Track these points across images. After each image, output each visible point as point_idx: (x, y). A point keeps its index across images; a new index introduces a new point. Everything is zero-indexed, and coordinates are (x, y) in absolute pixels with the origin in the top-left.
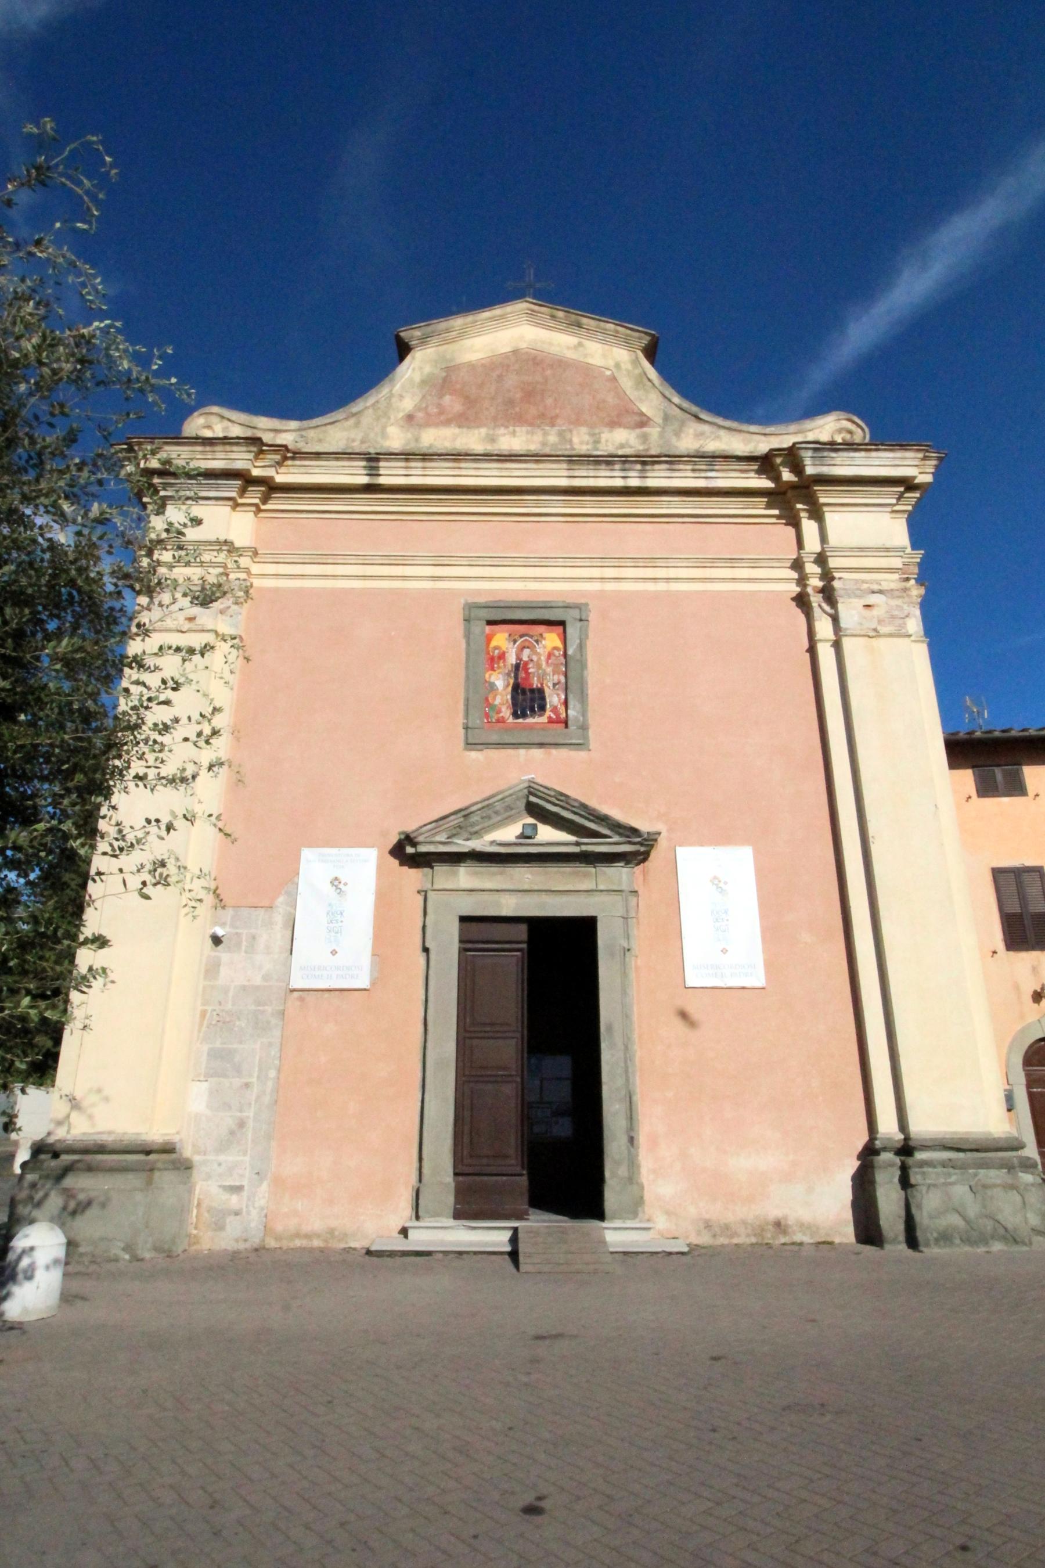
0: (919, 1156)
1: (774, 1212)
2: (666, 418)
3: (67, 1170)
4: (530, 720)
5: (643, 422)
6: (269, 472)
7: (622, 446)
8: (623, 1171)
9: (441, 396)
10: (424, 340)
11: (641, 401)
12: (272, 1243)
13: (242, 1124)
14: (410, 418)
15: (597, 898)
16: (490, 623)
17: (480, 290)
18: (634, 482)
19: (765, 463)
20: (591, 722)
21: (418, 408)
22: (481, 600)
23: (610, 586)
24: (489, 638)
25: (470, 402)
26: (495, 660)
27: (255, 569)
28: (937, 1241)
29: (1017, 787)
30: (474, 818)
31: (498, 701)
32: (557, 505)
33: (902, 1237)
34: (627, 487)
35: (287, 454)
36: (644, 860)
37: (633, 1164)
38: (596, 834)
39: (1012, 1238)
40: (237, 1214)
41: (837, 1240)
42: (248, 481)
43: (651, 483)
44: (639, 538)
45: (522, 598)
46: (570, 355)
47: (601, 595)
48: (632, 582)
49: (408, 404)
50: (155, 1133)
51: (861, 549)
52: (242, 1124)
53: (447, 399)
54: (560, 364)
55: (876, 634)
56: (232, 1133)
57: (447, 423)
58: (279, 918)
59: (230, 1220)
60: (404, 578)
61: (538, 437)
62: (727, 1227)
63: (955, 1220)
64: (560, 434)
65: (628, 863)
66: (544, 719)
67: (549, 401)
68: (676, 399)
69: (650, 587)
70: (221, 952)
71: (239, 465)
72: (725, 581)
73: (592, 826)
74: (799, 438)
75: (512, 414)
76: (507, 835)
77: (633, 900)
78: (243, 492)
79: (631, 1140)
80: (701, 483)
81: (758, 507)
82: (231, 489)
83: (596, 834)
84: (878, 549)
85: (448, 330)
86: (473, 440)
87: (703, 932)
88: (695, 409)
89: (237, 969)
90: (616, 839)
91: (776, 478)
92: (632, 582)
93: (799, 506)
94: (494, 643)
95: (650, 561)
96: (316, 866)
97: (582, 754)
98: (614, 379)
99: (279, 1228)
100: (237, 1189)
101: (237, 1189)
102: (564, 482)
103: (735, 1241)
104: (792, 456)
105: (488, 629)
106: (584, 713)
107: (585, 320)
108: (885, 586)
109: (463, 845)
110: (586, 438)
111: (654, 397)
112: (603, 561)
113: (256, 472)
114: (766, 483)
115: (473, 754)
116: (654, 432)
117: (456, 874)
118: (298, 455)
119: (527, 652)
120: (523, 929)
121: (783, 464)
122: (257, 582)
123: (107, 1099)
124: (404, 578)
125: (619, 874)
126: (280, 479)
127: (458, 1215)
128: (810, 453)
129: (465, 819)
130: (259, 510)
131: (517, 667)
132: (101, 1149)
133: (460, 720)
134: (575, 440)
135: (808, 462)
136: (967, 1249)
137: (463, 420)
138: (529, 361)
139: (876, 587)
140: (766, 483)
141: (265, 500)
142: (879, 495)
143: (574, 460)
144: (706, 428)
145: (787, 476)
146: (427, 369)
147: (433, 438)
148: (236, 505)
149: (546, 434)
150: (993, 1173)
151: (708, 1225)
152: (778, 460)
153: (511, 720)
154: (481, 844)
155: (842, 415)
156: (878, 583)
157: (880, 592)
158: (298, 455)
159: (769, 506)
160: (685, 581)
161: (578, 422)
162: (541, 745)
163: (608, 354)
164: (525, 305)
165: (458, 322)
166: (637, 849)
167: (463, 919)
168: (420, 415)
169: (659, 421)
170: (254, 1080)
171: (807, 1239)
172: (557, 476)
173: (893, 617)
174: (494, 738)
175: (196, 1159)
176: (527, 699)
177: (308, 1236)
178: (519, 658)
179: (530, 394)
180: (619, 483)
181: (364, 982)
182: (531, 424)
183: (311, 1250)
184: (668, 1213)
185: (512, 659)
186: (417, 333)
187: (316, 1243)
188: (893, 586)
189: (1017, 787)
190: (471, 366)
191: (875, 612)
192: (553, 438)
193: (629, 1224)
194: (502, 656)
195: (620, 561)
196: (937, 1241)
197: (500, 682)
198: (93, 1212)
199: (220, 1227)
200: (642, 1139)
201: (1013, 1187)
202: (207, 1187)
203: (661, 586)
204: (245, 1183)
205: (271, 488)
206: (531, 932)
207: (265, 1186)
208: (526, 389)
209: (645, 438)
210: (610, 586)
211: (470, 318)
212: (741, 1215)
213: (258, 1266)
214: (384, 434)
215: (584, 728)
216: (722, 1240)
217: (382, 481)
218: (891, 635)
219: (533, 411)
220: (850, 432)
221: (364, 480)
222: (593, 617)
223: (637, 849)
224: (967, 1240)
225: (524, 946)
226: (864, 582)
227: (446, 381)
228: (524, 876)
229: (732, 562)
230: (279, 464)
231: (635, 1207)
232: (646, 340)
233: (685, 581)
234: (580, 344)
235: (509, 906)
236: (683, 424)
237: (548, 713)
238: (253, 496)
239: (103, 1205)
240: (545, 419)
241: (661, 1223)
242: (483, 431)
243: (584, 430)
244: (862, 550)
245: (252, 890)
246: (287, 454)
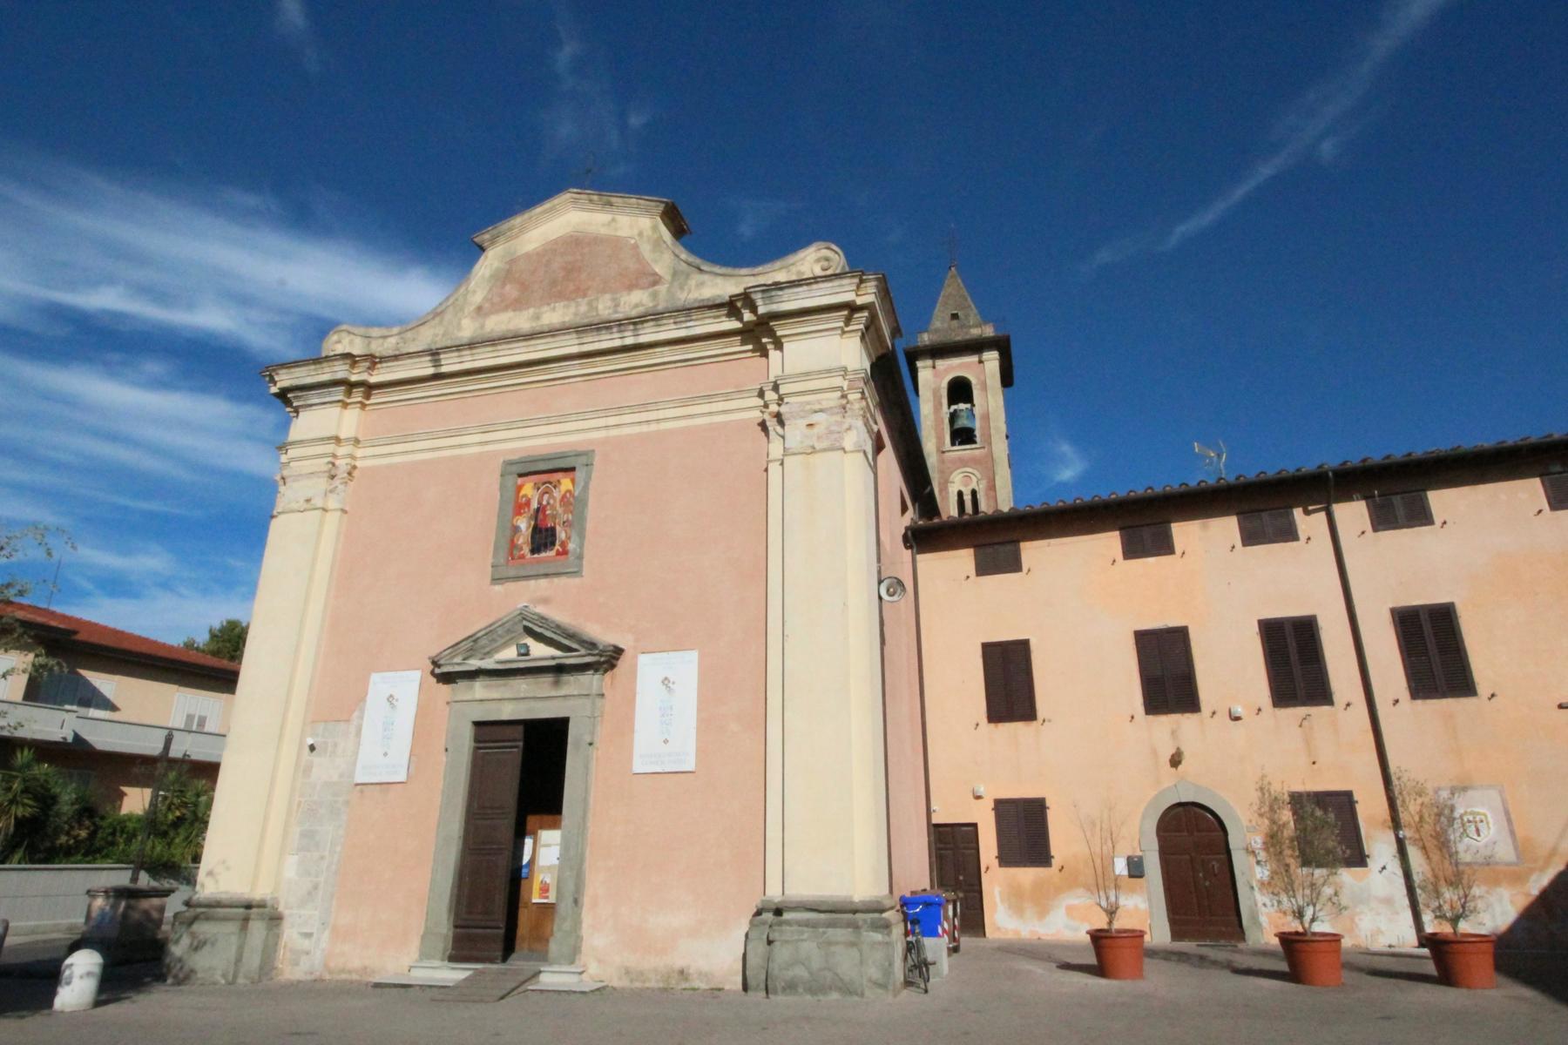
0: (787, 916)
1: (679, 962)
2: (675, 274)
3: (196, 918)
4: (543, 555)
5: (656, 280)
6: (364, 377)
7: (636, 306)
8: (567, 926)
9: (504, 284)
10: (493, 241)
11: (656, 261)
12: (327, 977)
13: (316, 887)
14: (479, 309)
15: (571, 702)
16: (521, 475)
17: (534, 191)
18: (629, 341)
19: (731, 307)
20: (586, 552)
21: (485, 299)
22: (515, 457)
23: (614, 432)
24: (519, 488)
25: (524, 287)
26: (520, 507)
27: (359, 453)
28: (784, 989)
29: (1014, 565)
30: (483, 642)
31: (521, 541)
32: (575, 369)
33: (763, 986)
34: (618, 345)
35: (373, 361)
36: (613, 666)
37: (577, 923)
38: (570, 649)
39: (847, 989)
40: (308, 953)
41: (727, 987)
42: (350, 386)
43: (643, 339)
44: (640, 387)
45: (544, 452)
46: (603, 231)
47: (606, 441)
48: (630, 426)
49: (478, 298)
50: (259, 893)
51: (807, 374)
52: (316, 887)
53: (508, 288)
54: (596, 240)
55: (814, 450)
56: (309, 893)
57: (506, 308)
58: (352, 729)
59: (304, 958)
60: (460, 446)
61: (572, 310)
62: (642, 973)
63: (800, 972)
64: (590, 304)
65: (596, 670)
66: (552, 553)
67: (584, 276)
68: (684, 256)
69: (645, 428)
70: (315, 758)
71: (340, 375)
72: (705, 415)
73: (566, 642)
74: (752, 282)
75: (557, 292)
76: (510, 653)
77: (599, 702)
78: (349, 394)
79: (576, 901)
80: (682, 333)
81: (735, 345)
82: (338, 393)
83: (570, 649)
84: (820, 372)
85: (510, 229)
86: (522, 321)
87: (649, 725)
88: (697, 261)
89: (324, 769)
90: (583, 651)
91: (740, 319)
92: (630, 426)
93: (764, 340)
94: (523, 492)
95: (644, 407)
96: (380, 684)
97: (577, 581)
98: (636, 247)
99: (332, 965)
100: (308, 935)
101: (308, 935)
102: (575, 350)
103: (647, 985)
104: (747, 298)
105: (520, 481)
106: (581, 546)
107: (614, 200)
108: (825, 405)
109: (474, 664)
110: (609, 303)
111: (667, 258)
112: (607, 411)
113: (354, 378)
114: (735, 324)
115: (498, 588)
116: (662, 289)
117: (471, 688)
118: (383, 359)
119: (546, 497)
120: (521, 728)
121: (745, 306)
122: (358, 464)
123: (228, 869)
124: (460, 446)
125: (590, 680)
126: (373, 380)
127: (452, 959)
128: (760, 295)
129: (473, 644)
130: (363, 406)
131: (538, 510)
132: (218, 904)
133: (490, 560)
134: (600, 307)
135: (759, 302)
136: (808, 997)
137: (517, 305)
138: (576, 241)
139: (817, 407)
140: (736, 325)
141: (368, 397)
142: (828, 321)
143: (581, 329)
144: (706, 277)
145: (748, 316)
146: (496, 264)
147: (498, 323)
148: (345, 405)
149: (578, 305)
150: (839, 931)
151: (628, 972)
152: (739, 304)
153: (529, 556)
154: (488, 664)
155: (822, 244)
156: (819, 402)
157: (821, 411)
158: (383, 359)
159: (743, 343)
160: (670, 419)
161: (604, 291)
162: (546, 575)
163: (635, 225)
164: (568, 196)
165: (517, 221)
166: (609, 659)
167: (477, 724)
168: (487, 305)
169: (668, 277)
170: (327, 853)
171: (703, 986)
172: (570, 345)
173: (831, 432)
174: (512, 573)
175: (286, 912)
176: (543, 538)
177: (350, 972)
178: (540, 503)
179: (571, 270)
180: (617, 343)
181: (402, 777)
182: (568, 299)
183: (352, 982)
184: (599, 961)
185: (535, 505)
186: (487, 236)
187: (355, 977)
188: (832, 404)
189: (1014, 565)
190: (528, 255)
191: (816, 430)
192: (583, 308)
193: (564, 969)
194: (528, 503)
195: (620, 410)
196: (784, 989)
197: (524, 524)
198: (207, 948)
199: (297, 964)
200: (586, 900)
201: (853, 944)
202: (290, 934)
203: (653, 427)
204: (314, 930)
205: (369, 388)
206: (526, 732)
207: (326, 934)
208: (570, 268)
209: (655, 296)
210: (614, 432)
211: (526, 216)
212: (654, 965)
213: (314, 990)
214: (459, 327)
215: (580, 557)
216: (638, 985)
217: (444, 369)
218: (825, 450)
219: (572, 287)
220: (827, 259)
221: (431, 371)
222: (597, 460)
223: (609, 659)
224: (812, 991)
225: (521, 744)
226: (808, 403)
227: (506, 276)
228: (522, 685)
229: (709, 398)
230: (373, 366)
231: (573, 955)
232: (662, 207)
233: (670, 419)
234: (613, 220)
235: (507, 712)
236: (688, 276)
237: (557, 547)
238: (357, 396)
239: (213, 944)
240: (581, 292)
241: (593, 969)
242: (531, 311)
243: (608, 296)
244: (807, 375)
245: (339, 704)
246: (373, 361)
